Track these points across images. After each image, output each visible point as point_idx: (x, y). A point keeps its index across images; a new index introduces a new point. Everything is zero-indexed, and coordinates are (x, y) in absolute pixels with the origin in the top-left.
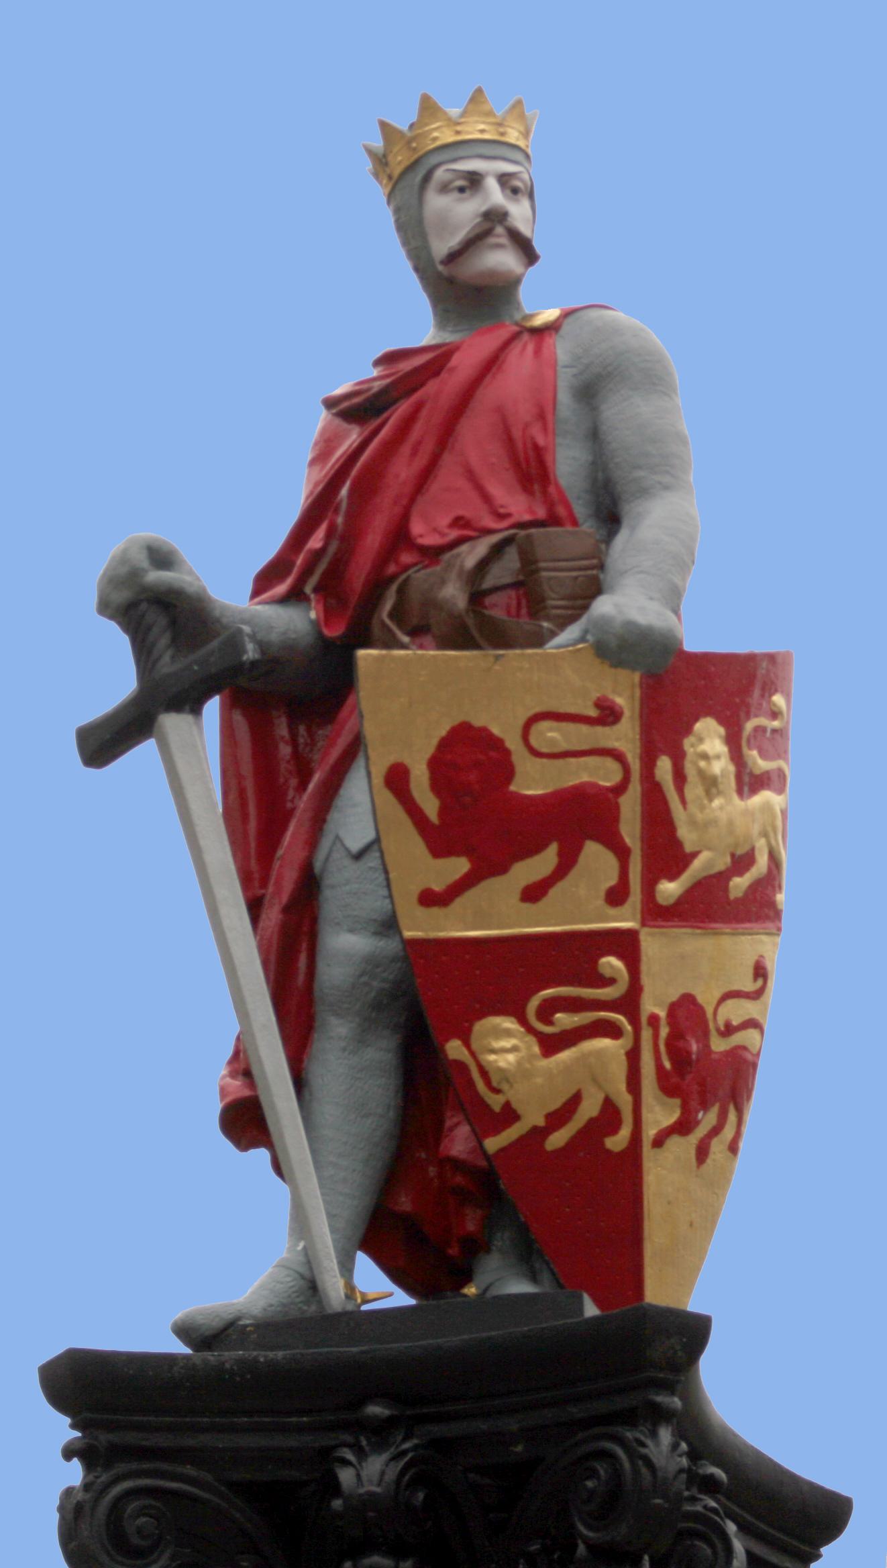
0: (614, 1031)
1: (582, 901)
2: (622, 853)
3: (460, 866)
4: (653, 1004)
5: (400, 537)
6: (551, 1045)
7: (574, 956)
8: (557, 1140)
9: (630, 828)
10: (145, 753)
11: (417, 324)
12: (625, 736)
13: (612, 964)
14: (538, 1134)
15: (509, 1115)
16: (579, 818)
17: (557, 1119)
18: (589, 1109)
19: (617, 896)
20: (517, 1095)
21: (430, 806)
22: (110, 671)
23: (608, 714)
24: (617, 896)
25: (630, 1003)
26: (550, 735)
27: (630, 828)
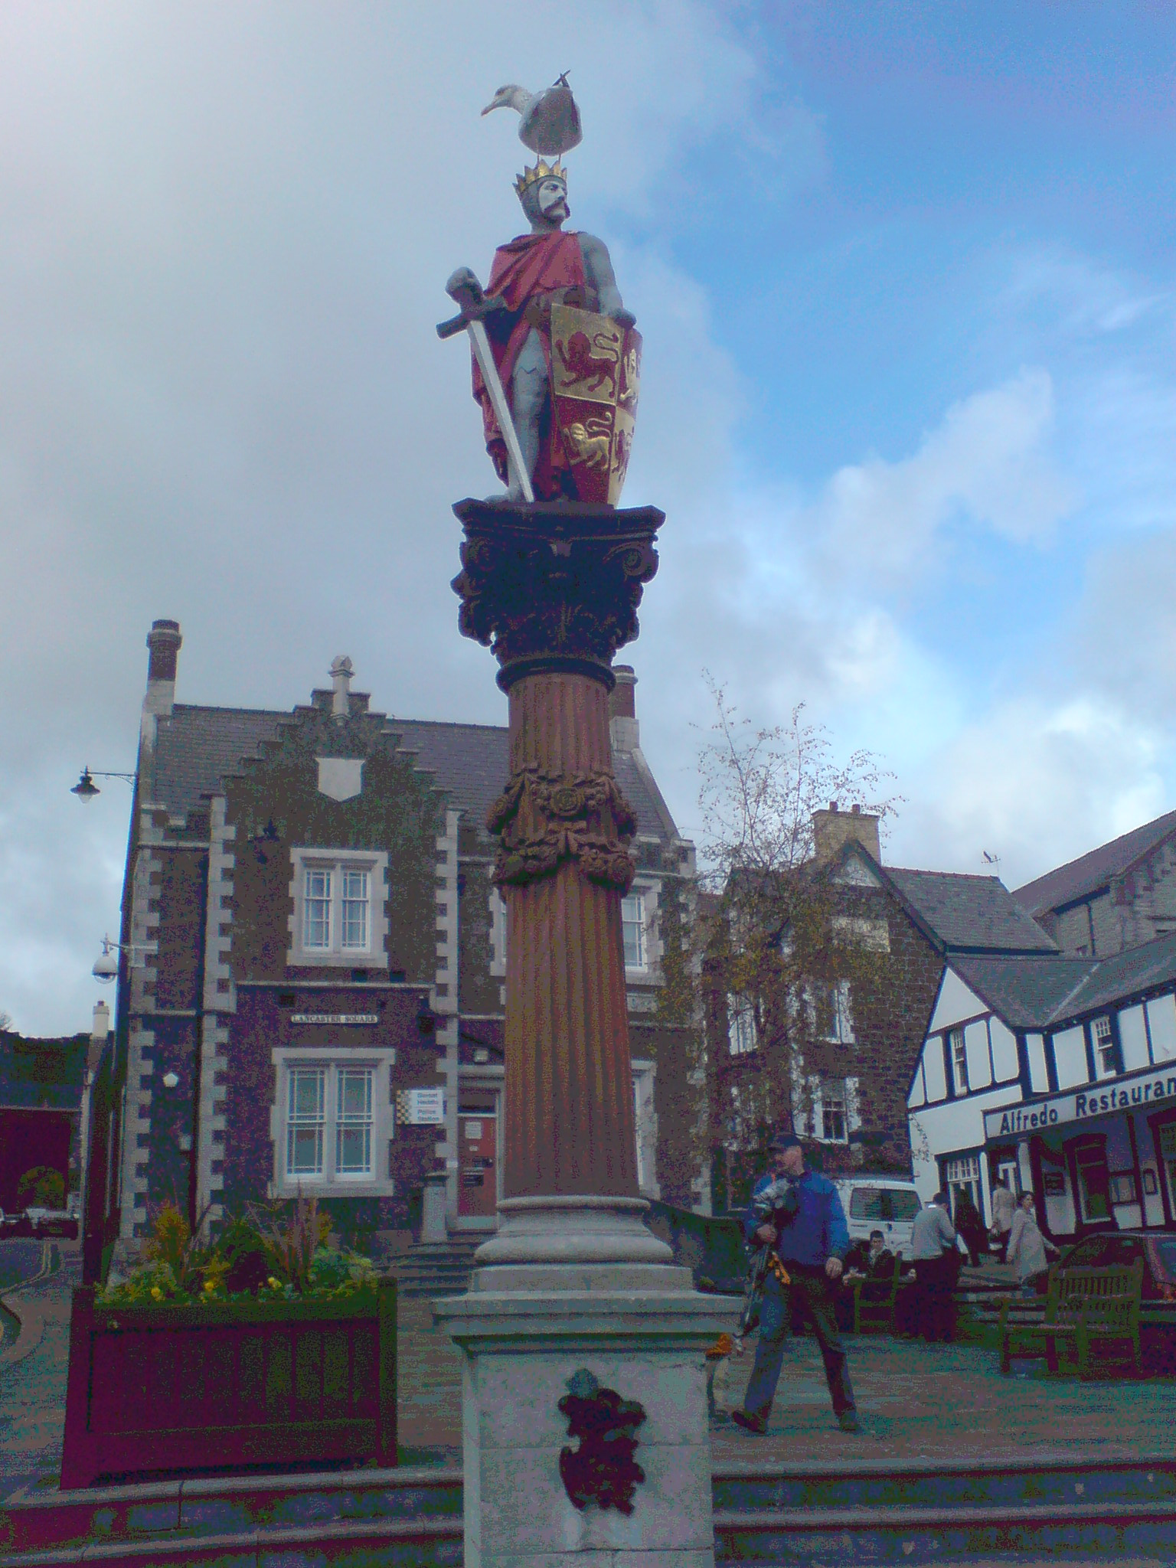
0: (607, 435)
1: (602, 395)
2: (614, 382)
3: (574, 375)
4: (616, 431)
5: (537, 284)
6: (592, 435)
7: (600, 409)
8: (590, 464)
9: (617, 376)
10: (463, 335)
11: (524, 227)
12: (617, 346)
13: (608, 414)
14: (584, 462)
15: (578, 454)
16: (605, 368)
17: (590, 458)
18: (598, 457)
19: (612, 395)
20: (581, 448)
21: (567, 357)
22: (453, 309)
23: (616, 339)
24: (612, 395)
25: (611, 427)
26: (600, 339)
27: (617, 376)
